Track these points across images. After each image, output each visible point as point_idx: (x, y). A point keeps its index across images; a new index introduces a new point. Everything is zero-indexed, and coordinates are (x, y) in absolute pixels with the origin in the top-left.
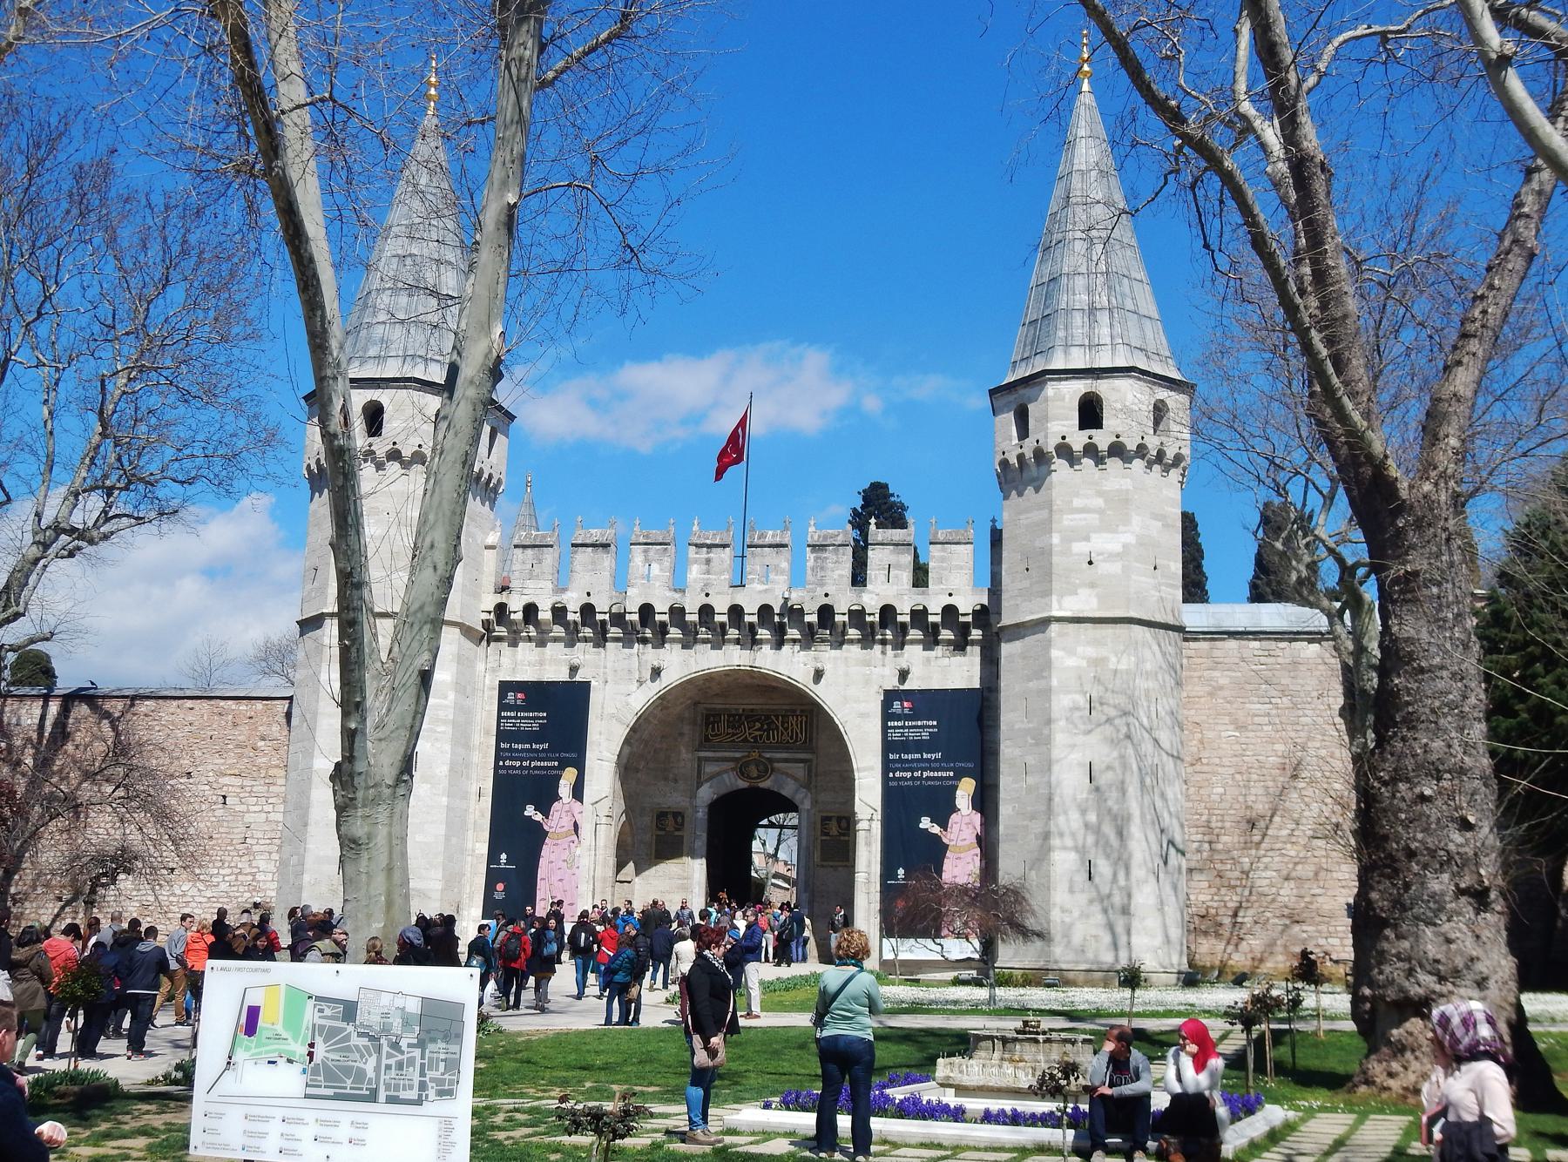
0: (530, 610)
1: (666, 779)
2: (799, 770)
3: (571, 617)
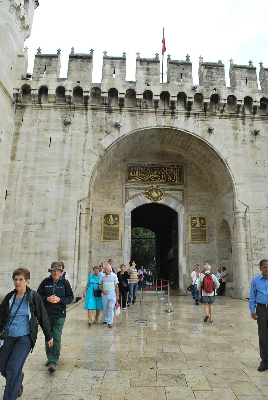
0: (44, 90)
1: (109, 198)
2: (178, 195)
3: (67, 93)
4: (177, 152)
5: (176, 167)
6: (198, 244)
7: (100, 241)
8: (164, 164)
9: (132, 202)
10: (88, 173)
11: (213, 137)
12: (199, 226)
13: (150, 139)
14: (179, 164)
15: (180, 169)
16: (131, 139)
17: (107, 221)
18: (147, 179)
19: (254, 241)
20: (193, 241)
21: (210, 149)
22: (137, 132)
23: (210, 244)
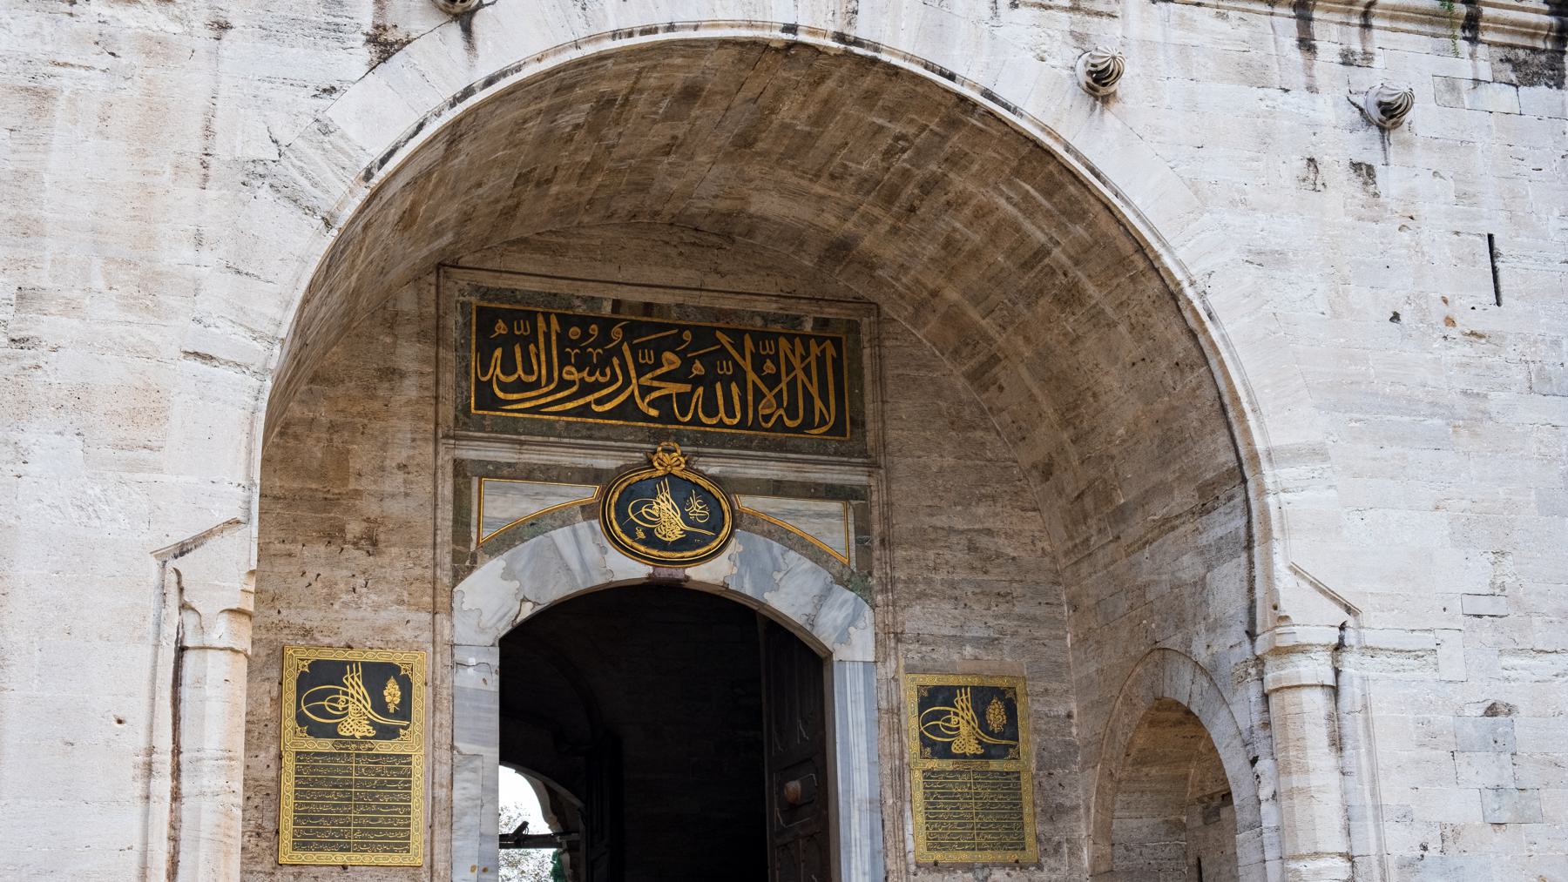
1: (333, 535)
2: (829, 526)
4: (833, 221)
5: (808, 327)
6: (970, 875)
7: (267, 865)
8: (728, 304)
9: (508, 574)
10: (241, 338)
11: (1118, 125)
12: (972, 748)
13: (667, 118)
14: (830, 312)
15: (837, 343)
16: (544, 105)
17: (321, 712)
18: (608, 407)
19: (1401, 842)
20: (938, 856)
21: (1098, 207)
22: (602, 57)
23: (1053, 870)
